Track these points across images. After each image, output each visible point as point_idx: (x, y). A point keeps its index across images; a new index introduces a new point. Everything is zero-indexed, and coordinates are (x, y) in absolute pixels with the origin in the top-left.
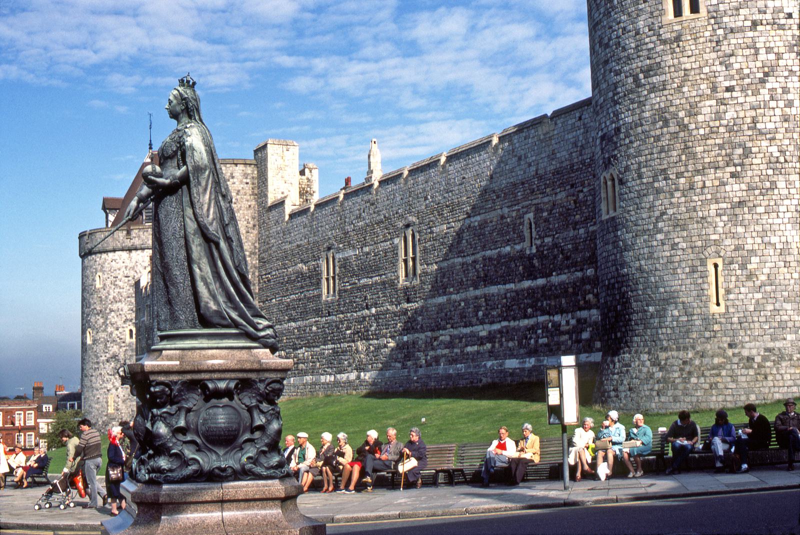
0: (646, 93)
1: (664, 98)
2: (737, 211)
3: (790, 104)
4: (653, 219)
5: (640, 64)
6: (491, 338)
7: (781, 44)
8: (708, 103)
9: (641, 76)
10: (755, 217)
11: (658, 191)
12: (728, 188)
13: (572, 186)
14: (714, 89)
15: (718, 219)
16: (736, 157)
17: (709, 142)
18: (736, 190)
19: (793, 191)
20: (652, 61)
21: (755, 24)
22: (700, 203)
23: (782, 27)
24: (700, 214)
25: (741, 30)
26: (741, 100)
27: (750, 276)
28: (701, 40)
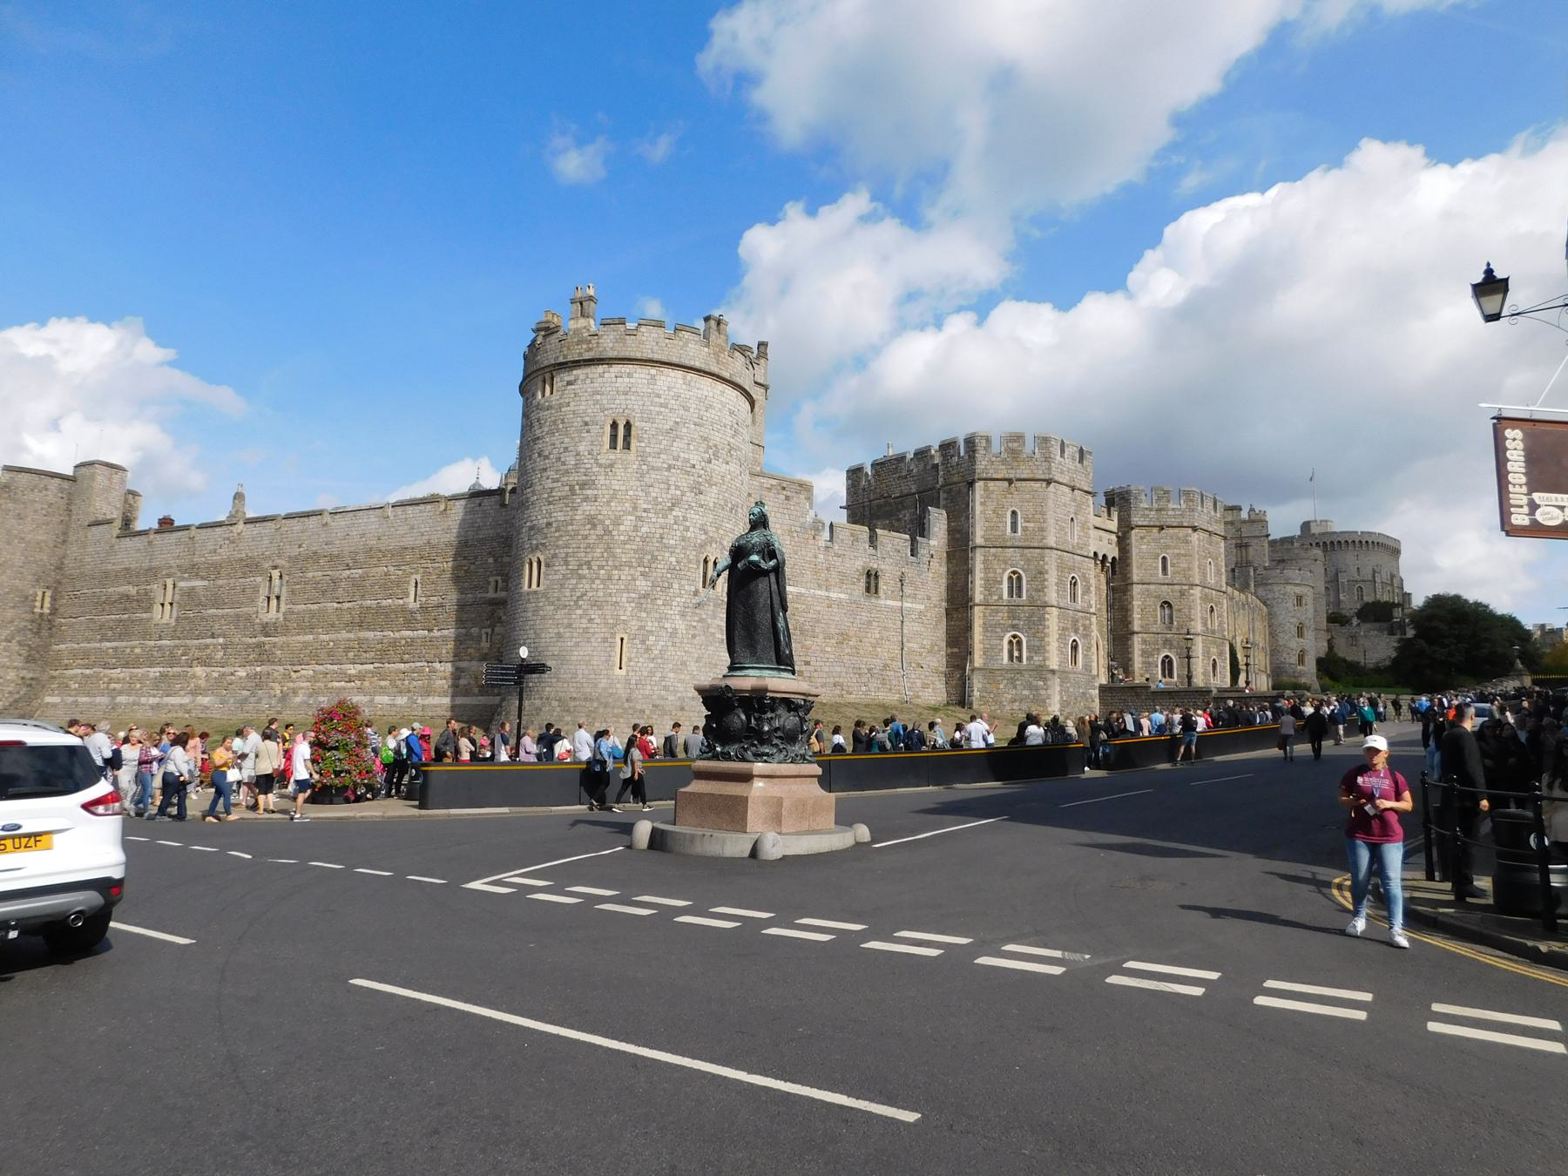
3: (687, 529)
6: (361, 677)
11: (581, 577)
14: (635, 508)
18: (642, 585)
21: (670, 468)
23: (688, 473)
25: (659, 469)
27: (648, 650)
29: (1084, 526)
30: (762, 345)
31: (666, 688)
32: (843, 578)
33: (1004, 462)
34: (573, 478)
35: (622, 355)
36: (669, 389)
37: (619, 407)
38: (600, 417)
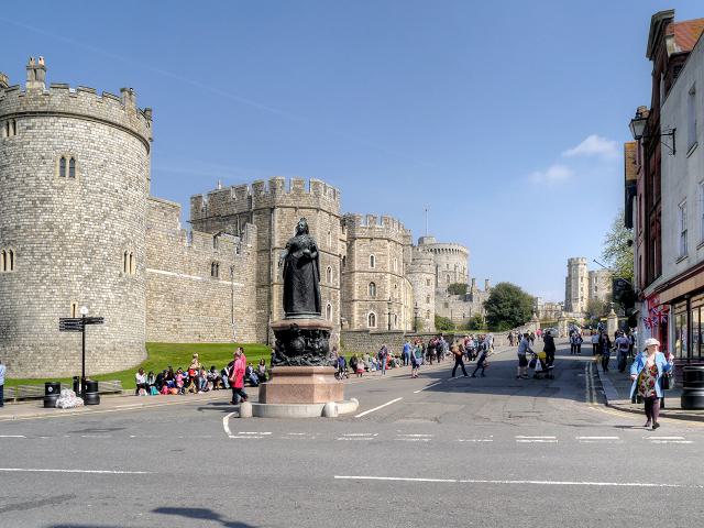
3: (114, 233)
14: (80, 218)
18: (86, 269)
21: (102, 191)
23: (113, 195)
25: (95, 192)
29: (335, 237)
33: (292, 196)
37: (66, 147)
38: (53, 154)
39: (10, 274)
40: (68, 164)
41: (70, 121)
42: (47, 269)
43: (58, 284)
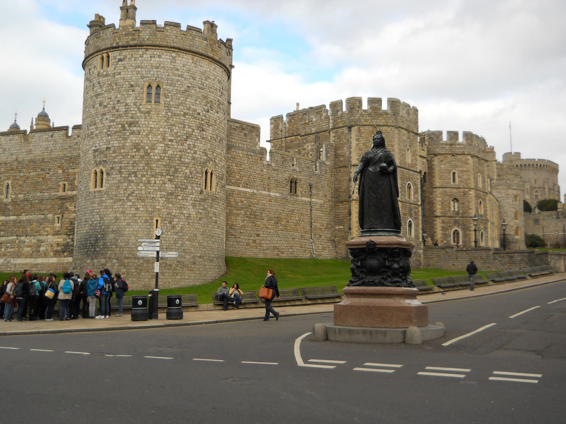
0: (128, 134)
1: (138, 138)
2: (170, 197)
3: (195, 153)
4: (126, 195)
5: (126, 120)
7: (194, 125)
8: (161, 145)
9: (126, 126)
10: (178, 201)
11: (131, 182)
12: (167, 185)
13: (42, 170)
14: (164, 139)
15: (160, 199)
16: (171, 172)
17: (159, 163)
18: (169, 186)
19: (194, 191)
20: (133, 120)
21: (185, 114)
22: (152, 190)
23: (195, 118)
24: (152, 196)
25: (179, 115)
26: (175, 146)
27: (173, 227)
28: (160, 115)
29: (414, 154)
30: (229, 40)
31: (184, 251)
32: (278, 184)
34: (124, 119)
35: (154, 43)
36: (184, 66)
39: (100, 191)
40: (154, 91)
41: (157, 52)
42: (133, 187)
43: (143, 201)
